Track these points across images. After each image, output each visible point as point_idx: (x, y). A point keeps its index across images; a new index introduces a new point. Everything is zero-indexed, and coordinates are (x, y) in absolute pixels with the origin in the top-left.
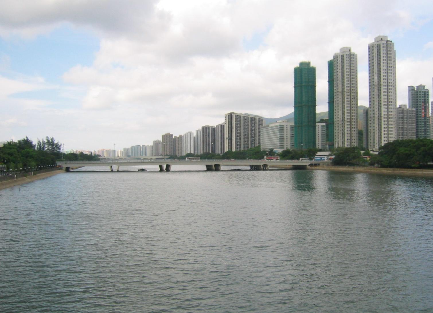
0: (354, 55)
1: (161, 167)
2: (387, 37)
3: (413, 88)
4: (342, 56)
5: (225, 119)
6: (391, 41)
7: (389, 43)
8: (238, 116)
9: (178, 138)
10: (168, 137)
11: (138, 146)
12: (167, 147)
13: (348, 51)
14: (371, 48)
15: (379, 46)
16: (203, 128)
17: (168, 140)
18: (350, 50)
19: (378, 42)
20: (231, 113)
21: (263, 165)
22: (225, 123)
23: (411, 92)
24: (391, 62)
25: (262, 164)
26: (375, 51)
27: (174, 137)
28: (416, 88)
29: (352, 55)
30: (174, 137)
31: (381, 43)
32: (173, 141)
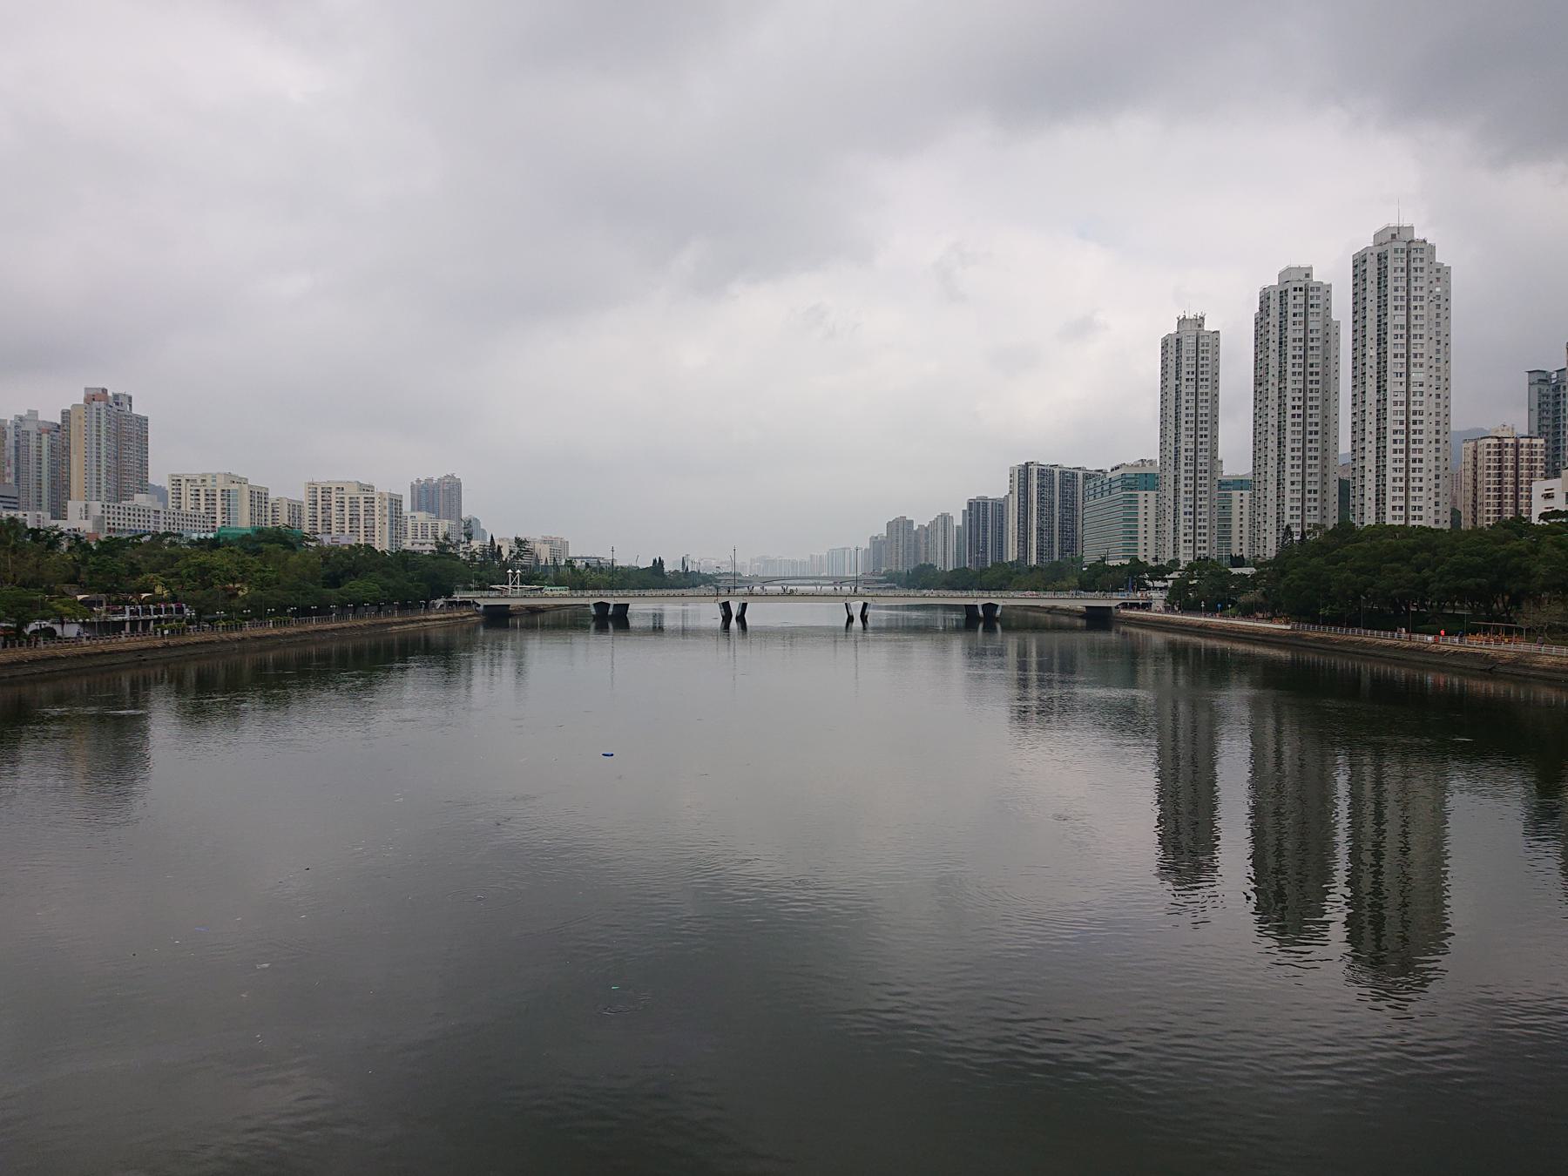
0: (1318, 289)
1: (726, 606)
2: (1412, 228)
3: (1543, 377)
4: (1281, 293)
5: (1011, 481)
6: (1425, 241)
7: (1413, 245)
8: (1045, 474)
9: (926, 529)
10: (901, 526)
11: (845, 549)
12: (897, 553)
13: (1303, 278)
14: (1359, 262)
15: (1381, 258)
16: (970, 504)
17: (901, 534)
18: (1307, 276)
19: (1381, 244)
20: (1027, 463)
21: (984, 606)
22: (1011, 492)
23: (1535, 388)
24: (1423, 303)
25: (980, 603)
26: (1372, 275)
27: (915, 528)
28: (1554, 376)
29: (1312, 289)
30: (915, 528)
31: (1390, 248)
32: (913, 536)
